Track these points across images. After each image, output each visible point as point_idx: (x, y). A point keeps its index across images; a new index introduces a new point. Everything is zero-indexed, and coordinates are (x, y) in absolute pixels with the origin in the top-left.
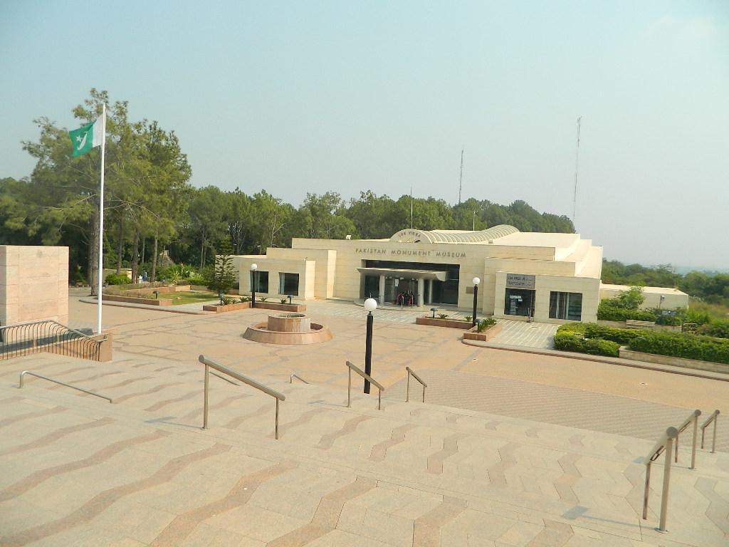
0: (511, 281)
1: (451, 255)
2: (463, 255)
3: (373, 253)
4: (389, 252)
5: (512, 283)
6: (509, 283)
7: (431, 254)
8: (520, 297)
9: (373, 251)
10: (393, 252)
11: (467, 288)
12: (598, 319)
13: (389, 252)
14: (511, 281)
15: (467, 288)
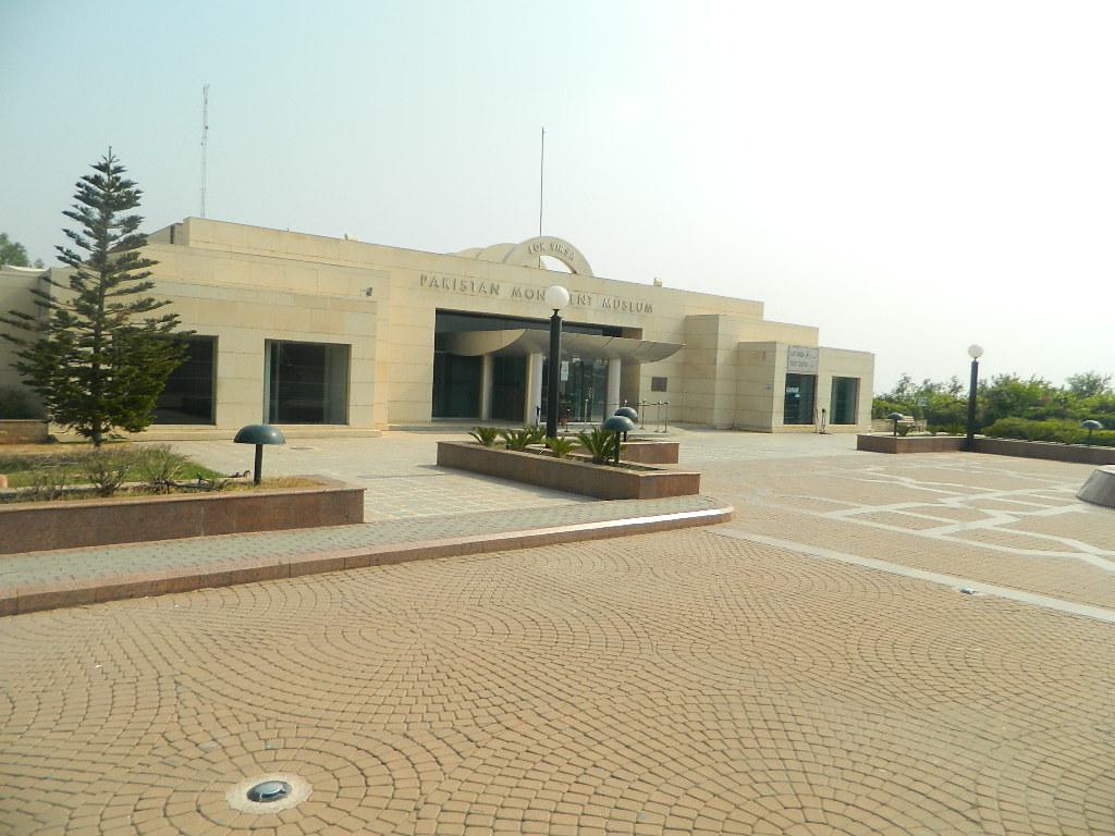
0: (792, 358)
1: (628, 305)
2: (648, 309)
3: (469, 291)
4: (505, 292)
5: (793, 363)
6: (790, 363)
7: (594, 304)
8: (797, 390)
9: (468, 285)
10: (515, 293)
11: (654, 379)
12: (873, 418)
13: (505, 292)
14: (792, 358)
15: (654, 379)
